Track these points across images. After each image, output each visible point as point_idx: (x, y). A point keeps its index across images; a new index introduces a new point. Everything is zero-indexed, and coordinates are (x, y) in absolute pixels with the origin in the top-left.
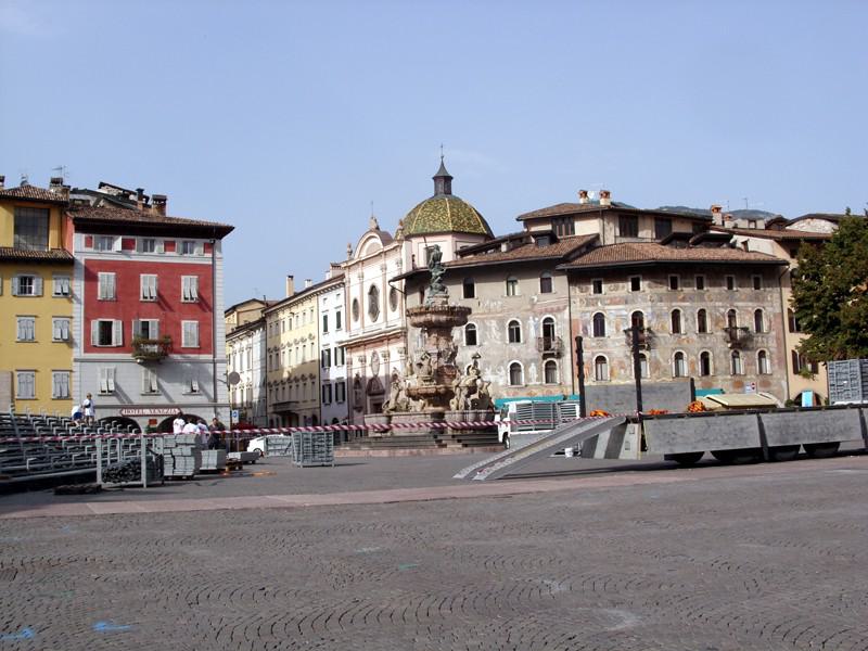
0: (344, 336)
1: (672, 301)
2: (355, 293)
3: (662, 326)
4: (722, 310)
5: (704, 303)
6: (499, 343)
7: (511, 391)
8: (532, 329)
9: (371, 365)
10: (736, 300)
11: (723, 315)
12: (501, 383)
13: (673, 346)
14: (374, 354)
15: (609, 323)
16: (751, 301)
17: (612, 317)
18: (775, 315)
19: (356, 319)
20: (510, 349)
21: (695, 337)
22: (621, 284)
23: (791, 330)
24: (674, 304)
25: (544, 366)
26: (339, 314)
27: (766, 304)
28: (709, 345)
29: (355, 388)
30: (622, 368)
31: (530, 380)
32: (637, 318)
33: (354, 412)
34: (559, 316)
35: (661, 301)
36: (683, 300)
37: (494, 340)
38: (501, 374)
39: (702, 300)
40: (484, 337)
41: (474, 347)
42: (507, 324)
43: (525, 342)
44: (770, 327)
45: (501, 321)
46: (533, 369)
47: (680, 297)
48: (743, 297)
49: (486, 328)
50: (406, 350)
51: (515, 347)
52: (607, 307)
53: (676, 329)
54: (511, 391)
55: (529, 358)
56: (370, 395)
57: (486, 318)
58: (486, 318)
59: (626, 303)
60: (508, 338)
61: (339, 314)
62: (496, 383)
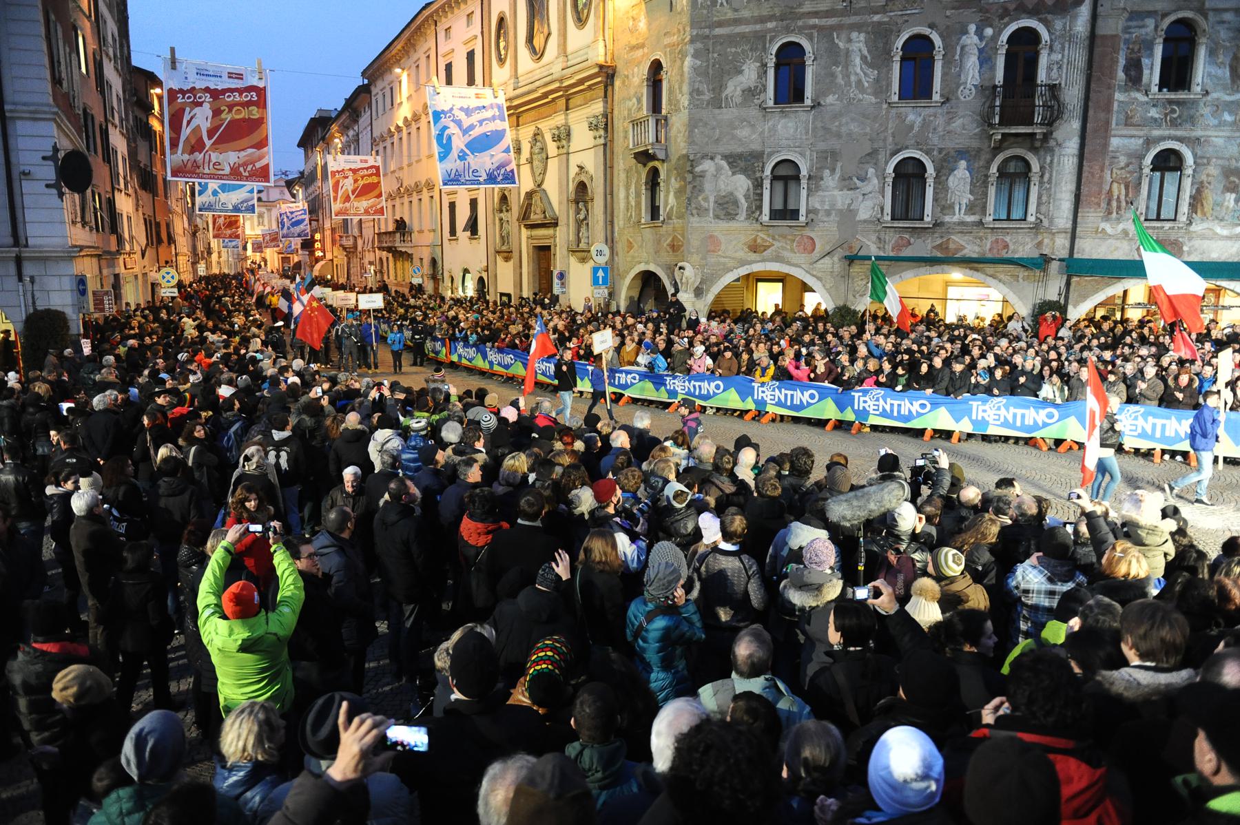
6: (873, 100)
8: (972, 62)
9: (530, 161)
12: (865, 212)
14: (537, 136)
15: (1212, 53)
19: (501, 61)
25: (994, 169)
26: (471, 56)
29: (501, 211)
31: (947, 208)
34: (1058, 24)
37: (853, 92)
38: (867, 188)
40: (827, 83)
41: (796, 107)
42: (900, 43)
43: (946, 100)
45: (880, 37)
46: (960, 177)
49: (835, 56)
51: (914, 115)
54: (891, 238)
55: (950, 145)
57: (839, 28)
60: (896, 87)
61: (471, 56)
62: (848, 214)
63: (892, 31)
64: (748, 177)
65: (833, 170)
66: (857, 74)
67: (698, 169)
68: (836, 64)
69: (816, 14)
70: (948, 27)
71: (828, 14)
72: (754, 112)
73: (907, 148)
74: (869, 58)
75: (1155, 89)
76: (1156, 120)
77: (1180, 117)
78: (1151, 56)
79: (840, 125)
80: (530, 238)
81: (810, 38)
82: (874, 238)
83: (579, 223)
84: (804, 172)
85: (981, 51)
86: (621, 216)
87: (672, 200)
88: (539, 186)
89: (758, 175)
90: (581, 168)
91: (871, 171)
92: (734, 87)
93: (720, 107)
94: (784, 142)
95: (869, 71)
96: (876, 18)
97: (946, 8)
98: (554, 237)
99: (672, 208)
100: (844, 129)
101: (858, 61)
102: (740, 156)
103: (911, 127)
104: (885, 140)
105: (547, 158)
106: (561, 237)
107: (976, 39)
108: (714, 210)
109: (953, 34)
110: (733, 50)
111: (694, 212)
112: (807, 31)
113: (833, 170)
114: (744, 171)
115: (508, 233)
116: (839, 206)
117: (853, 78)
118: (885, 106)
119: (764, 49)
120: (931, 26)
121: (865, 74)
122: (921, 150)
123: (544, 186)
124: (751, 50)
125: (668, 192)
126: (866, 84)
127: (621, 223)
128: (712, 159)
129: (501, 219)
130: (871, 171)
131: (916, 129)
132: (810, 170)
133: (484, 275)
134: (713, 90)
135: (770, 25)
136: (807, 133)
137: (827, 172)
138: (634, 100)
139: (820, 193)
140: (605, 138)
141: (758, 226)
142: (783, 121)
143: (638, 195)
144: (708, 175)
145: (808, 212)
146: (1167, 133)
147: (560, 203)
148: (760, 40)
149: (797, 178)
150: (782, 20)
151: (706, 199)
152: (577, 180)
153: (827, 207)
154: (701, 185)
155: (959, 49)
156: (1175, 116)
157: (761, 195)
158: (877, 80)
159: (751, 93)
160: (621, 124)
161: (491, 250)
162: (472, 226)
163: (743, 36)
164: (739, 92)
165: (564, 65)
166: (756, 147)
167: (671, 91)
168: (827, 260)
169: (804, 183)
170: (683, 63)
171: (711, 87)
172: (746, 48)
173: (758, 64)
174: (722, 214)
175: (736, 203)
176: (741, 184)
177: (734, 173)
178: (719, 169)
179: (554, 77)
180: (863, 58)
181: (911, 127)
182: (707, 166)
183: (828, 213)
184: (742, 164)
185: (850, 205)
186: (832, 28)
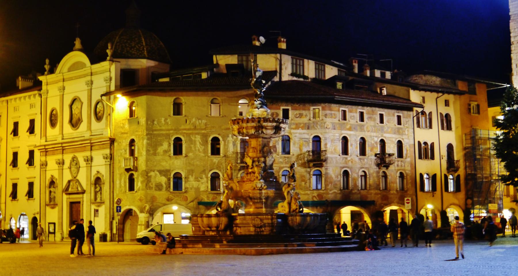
0: (36, 140)
1: (341, 130)
2: (53, 103)
3: (335, 149)
4: (376, 139)
5: (364, 133)
6: (203, 155)
7: (211, 196)
8: (231, 145)
10: (385, 133)
11: (376, 143)
12: (203, 188)
13: (341, 165)
14: (74, 159)
15: (294, 144)
16: (395, 133)
17: (297, 140)
18: (410, 146)
20: (212, 160)
21: (357, 159)
22: (304, 112)
23: (420, 158)
24: (343, 132)
27: (404, 137)
28: (367, 166)
30: (303, 181)
32: (317, 140)
33: (48, 208)
35: (335, 129)
36: (350, 129)
37: (197, 152)
38: (203, 181)
39: (362, 128)
40: (189, 149)
41: (180, 156)
44: (407, 154)
45: (205, 137)
47: (348, 127)
48: (390, 130)
49: (191, 142)
50: (111, 157)
51: (216, 159)
52: (292, 131)
53: (345, 151)
54: (211, 196)
56: (66, 194)
57: (192, 134)
58: (192, 134)
59: (308, 128)
62: (197, 189)
63: (207, 136)
64: (166, 177)
65: (192, 176)
66: (198, 147)
67: (149, 175)
68: (192, 144)
69: (185, 129)
70: (223, 135)
71: (189, 129)
72: (168, 158)
73: (214, 169)
74: (201, 143)
75: (280, 154)
76: (281, 162)
77: (288, 161)
78: (278, 144)
79: (194, 162)
80: (67, 199)
81: (184, 136)
82: (206, 196)
83: (96, 193)
84: (183, 176)
85: (233, 142)
86: (117, 190)
87: (139, 184)
88: (75, 178)
89: (169, 177)
90: (98, 172)
91: (204, 176)
92: (160, 150)
93: (156, 155)
94: (177, 167)
95: (202, 146)
96: (203, 131)
97: (222, 130)
98: (83, 198)
99: (140, 187)
100: (195, 163)
101: (198, 143)
102: (163, 171)
103: (215, 163)
104: (207, 167)
105: (80, 167)
106: (86, 199)
107: (231, 139)
108: (155, 188)
109: (225, 137)
110: (160, 138)
111: (148, 188)
112: (183, 134)
113: (192, 176)
114: (164, 176)
115: (55, 197)
116: (195, 186)
117: (197, 148)
118: (207, 157)
119: (170, 139)
120: (219, 135)
121: (201, 148)
122: (218, 170)
123: (78, 178)
124: (166, 139)
125: (138, 182)
126: (201, 150)
127: (117, 192)
128: (154, 171)
129: (50, 192)
130: (204, 176)
131: (216, 164)
132: (185, 176)
133: (38, 217)
134: (154, 150)
135: (171, 132)
136: (184, 164)
137: (190, 176)
138: (123, 151)
139: (189, 183)
140: (110, 162)
141: (169, 193)
142: (176, 160)
143: (125, 182)
144: (153, 177)
145: (185, 188)
146: (285, 165)
147: (87, 185)
148: (168, 136)
149: (181, 179)
150: (175, 131)
151: (152, 184)
152: (96, 177)
153: (191, 187)
154: (151, 179)
155: (227, 141)
156: (286, 161)
157: (170, 183)
158: (204, 149)
159: (165, 152)
160: (116, 158)
161: (43, 204)
162: (30, 194)
163: (163, 134)
164: (162, 151)
165: (90, 134)
166: (168, 168)
167: (139, 149)
168: (192, 203)
169: (183, 179)
170: (143, 141)
171: (153, 149)
172: (164, 138)
173: (168, 143)
174: (157, 189)
175: (162, 185)
176: (163, 180)
177: (161, 176)
178: (156, 175)
179: (85, 138)
180: (200, 143)
181: (215, 163)
182: (152, 174)
183: (191, 189)
184: (164, 173)
185: (198, 186)
186: (190, 134)
